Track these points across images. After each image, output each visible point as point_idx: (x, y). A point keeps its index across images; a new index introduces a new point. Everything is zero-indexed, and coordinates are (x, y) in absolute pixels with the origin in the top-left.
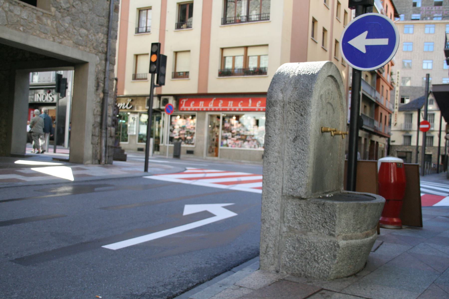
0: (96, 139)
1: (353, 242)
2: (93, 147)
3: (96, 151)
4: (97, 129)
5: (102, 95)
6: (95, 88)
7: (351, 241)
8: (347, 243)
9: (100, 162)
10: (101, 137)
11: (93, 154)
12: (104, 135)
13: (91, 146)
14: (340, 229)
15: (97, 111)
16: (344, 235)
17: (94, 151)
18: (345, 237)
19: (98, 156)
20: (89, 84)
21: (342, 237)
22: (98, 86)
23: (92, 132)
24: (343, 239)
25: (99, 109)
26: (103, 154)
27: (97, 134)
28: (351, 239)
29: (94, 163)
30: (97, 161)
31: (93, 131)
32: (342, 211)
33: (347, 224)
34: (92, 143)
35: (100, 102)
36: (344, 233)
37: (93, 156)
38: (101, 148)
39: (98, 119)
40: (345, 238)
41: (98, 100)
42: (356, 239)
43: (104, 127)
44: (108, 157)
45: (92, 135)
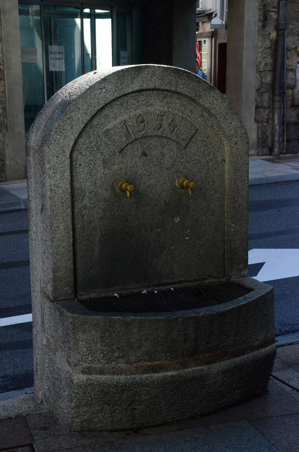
0: (265, 113)
1: (96, 377)
2: (258, 127)
3: (264, 133)
4: (266, 96)
5: (274, 35)
6: (260, 24)
7: (99, 376)
8: (87, 380)
9: (271, 151)
10: (272, 108)
11: (258, 138)
12: (277, 105)
13: (255, 126)
14: (79, 357)
15: (266, 64)
16: (85, 365)
17: (260, 133)
18: (88, 368)
19: (269, 141)
20: (246, 19)
21: (81, 367)
22: (265, 19)
23: (256, 101)
24: (83, 372)
25: (269, 60)
26: (276, 138)
27: (265, 104)
28: (101, 372)
29: (260, 154)
30: (266, 150)
31: (259, 100)
32: (78, 328)
33: (90, 350)
34: (256, 121)
35: (270, 47)
36: (85, 362)
37: (258, 142)
38: (273, 127)
39: (268, 79)
40: (87, 371)
41: (268, 43)
42: (113, 373)
43: (277, 92)
44: (287, 141)
45: (257, 108)
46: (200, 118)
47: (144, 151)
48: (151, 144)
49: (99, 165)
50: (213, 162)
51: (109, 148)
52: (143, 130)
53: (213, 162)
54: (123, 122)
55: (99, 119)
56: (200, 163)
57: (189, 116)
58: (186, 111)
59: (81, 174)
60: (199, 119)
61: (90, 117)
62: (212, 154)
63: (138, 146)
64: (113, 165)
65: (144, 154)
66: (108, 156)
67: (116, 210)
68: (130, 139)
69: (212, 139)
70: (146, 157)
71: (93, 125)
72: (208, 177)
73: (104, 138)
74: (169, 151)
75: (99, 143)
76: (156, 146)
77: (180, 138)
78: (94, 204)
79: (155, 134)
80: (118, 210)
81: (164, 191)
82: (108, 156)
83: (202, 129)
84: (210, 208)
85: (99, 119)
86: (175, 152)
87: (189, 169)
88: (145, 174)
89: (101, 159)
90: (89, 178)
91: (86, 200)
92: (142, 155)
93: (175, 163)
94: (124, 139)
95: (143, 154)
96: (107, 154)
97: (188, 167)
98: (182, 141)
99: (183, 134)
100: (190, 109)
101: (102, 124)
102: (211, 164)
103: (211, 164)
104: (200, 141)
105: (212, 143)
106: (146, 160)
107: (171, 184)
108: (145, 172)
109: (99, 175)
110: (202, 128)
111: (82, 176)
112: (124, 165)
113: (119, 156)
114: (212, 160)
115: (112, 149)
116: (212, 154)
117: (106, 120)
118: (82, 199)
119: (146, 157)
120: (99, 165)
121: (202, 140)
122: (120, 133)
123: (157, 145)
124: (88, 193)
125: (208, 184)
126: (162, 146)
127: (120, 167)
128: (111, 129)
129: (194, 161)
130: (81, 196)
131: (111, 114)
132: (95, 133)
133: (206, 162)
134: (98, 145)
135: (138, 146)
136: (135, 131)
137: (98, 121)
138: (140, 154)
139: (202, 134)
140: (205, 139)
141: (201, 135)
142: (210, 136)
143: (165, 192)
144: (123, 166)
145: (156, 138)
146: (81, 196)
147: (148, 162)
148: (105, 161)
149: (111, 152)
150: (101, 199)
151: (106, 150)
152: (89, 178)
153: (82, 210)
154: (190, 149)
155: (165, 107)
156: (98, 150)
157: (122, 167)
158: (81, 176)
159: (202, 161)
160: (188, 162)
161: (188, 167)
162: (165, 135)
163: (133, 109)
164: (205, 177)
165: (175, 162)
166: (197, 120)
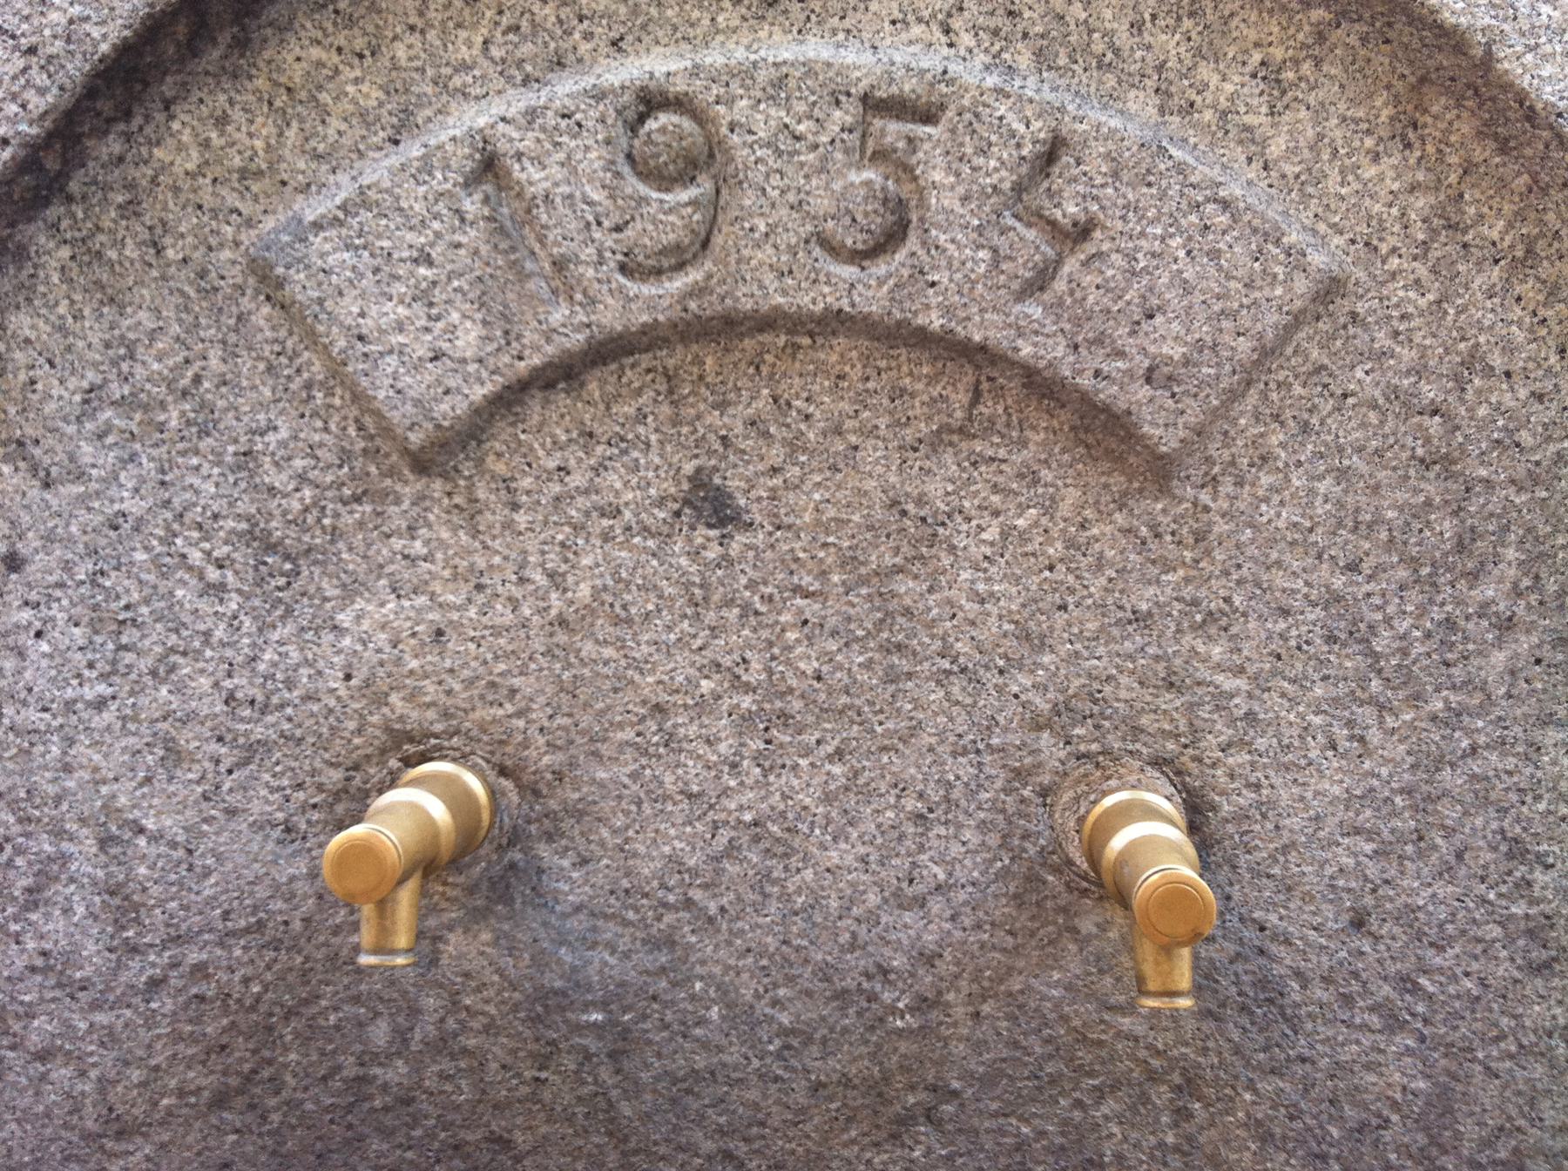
46: (1376, 158)
47: (699, 470)
48: (789, 404)
49: (213, 574)
50: (1525, 643)
51: (315, 414)
52: (678, 258)
53: (1525, 643)
54: (463, 159)
55: (222, 121)
56: (1360, 635)
57: (1247, 128)
58: (1214, 80)
59: (21, 654)
60: (1370, 172)
61: (61, 78)
62: (1511, 554)
63: (641, 417)
64: (349, 592)
65: (710, 505)
66: (307, 493)
67: (380, 1033)
68: (529, 337)
69: (1523, 393)
70: (723, 540)
71: (154, 181)
72: (1445, 794)
73: (266, 310)
74: (996, 489)
75: (214, 362)
76: (838, 431)
77: (1121, 354)
78: (152, 958)
79: (811, 300)
80: (401, 1036)
81: (921, 902)
82: (307, 493)
83: (1393, 276)
84: (1468, 1128)
85: (222, 121)
86: (1065, 509)
87: (1221, 699)
88: (702, 707)
89: (231, 524)
90: (100, 704)
91: (68, 911)
92: (678, 514)
93: (1060, 618)
94: (468, 339)
95: (687, 502)
96: (302, 478)
97: (1219, 678)
98: (1145, 392)
99: (1159, 319)
100: (1257, 57)
101: (244, 174)
102: (1499, 658)
103: (1499, 658)
104: (1374, 406)
105: (1525, 437)
106: (726, 561)
107: (993, 840)
108: (706, 685)
109: (204, 682)
110: (1394, 262)
111: (28, 675)
112: (480, 599)
113: (419, 499)
114: (1507, 625)
115: (352, 431)
116: (1511, 554)
117: (292, 133)
118: (29, 890)
119: (723, 540)
120: (213, 574)
121: (1394, 393)
122: (422, 271)
123: (849, 424)
124: (91, 846)
125: (1446, 872)
126: (909, 434)
127: (434, 616)
128: (317, 226)
129: (1285, 612)
130: (19, 861)
131: (349, 74)
132: (170, 253)
133: (1428, 635)
134: (197, 380)
135: (641, 417)
136: (591, 250)
137: (206, 144)
138: (661, 502)
139: (1397, 333)
140: (1429, 392)
141: (1382, 339)
142: (1497, 361)
143: (936, 905)
144: (472, 612)
145: (841, 342)
146: (19, 861)
147: (752, 585)
148: (271, 548)
149: (345, 456)
150: (226, 915)
151: (284, 433)
152: (100, 704)
153: (30, 1004)
154: (1239, 483)
155: (957, 23)
156: (204, 433)
157: (455, 616)
158: (19, 672)
159: (1388, 621)
160: (1213, 622)
161: (1219, 678)
162: (935, 321)
163: (588, 36)
164: (1408, 791)
165: (1063, 608)
166: (1335, 176)
